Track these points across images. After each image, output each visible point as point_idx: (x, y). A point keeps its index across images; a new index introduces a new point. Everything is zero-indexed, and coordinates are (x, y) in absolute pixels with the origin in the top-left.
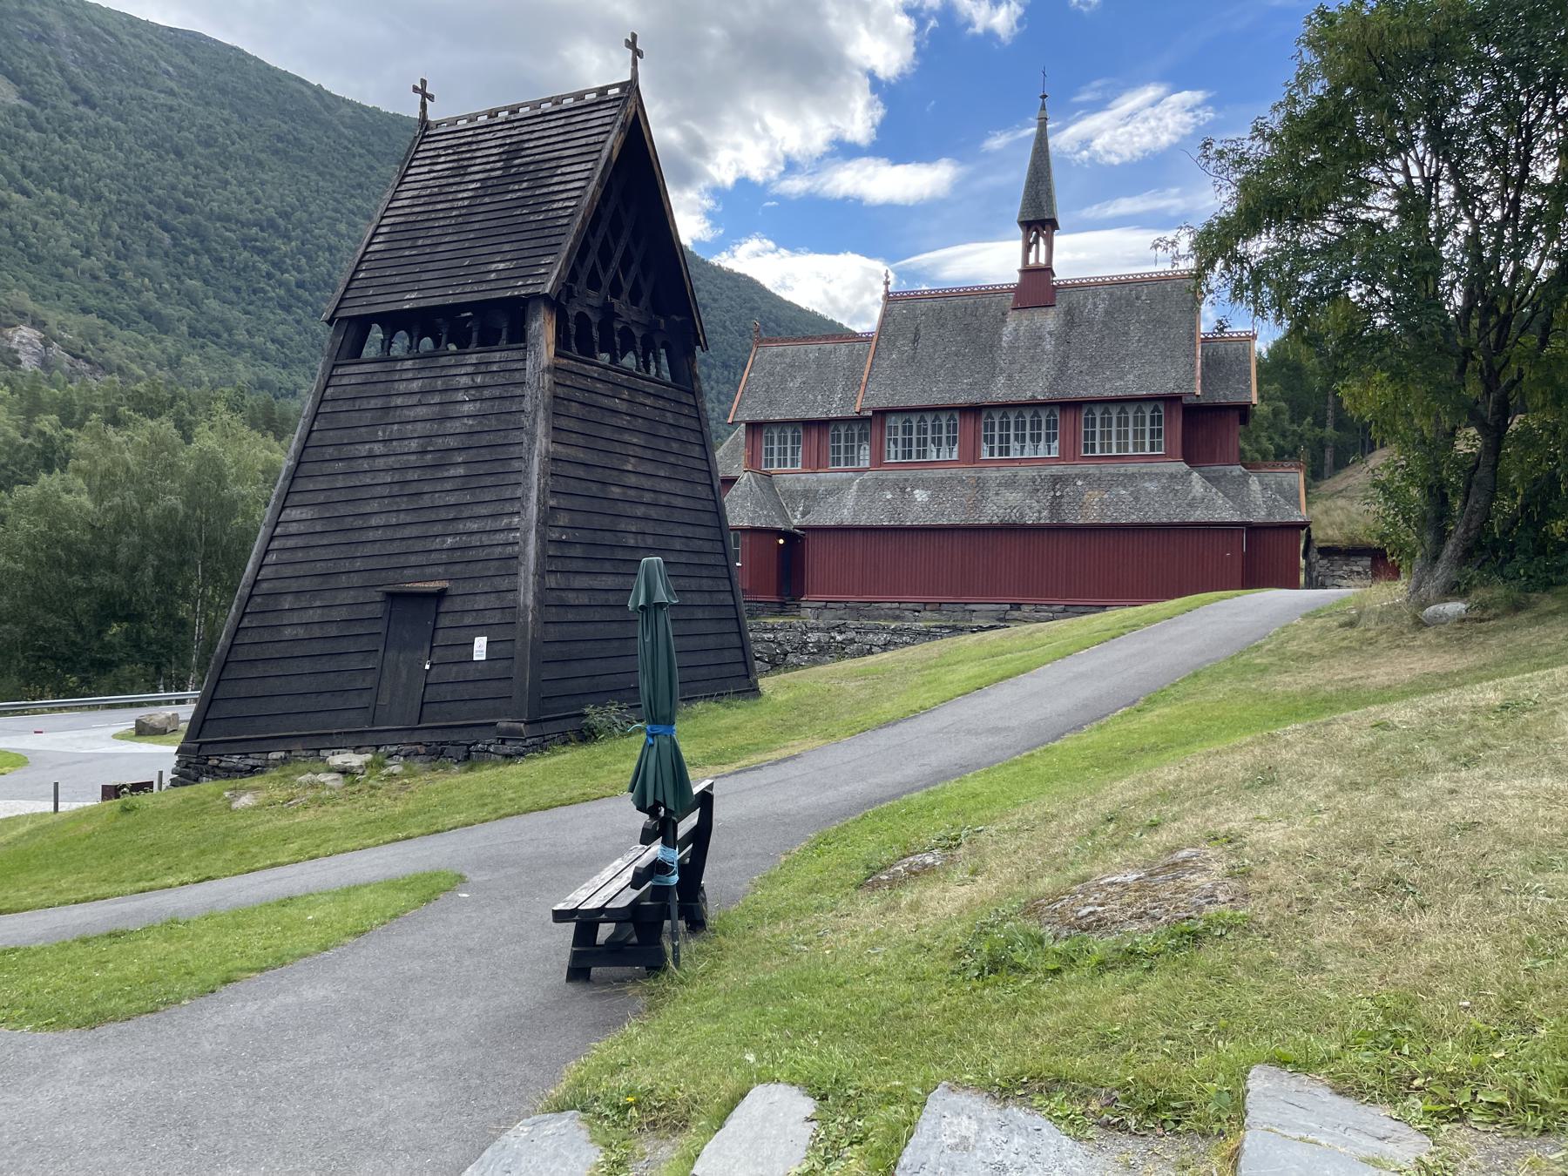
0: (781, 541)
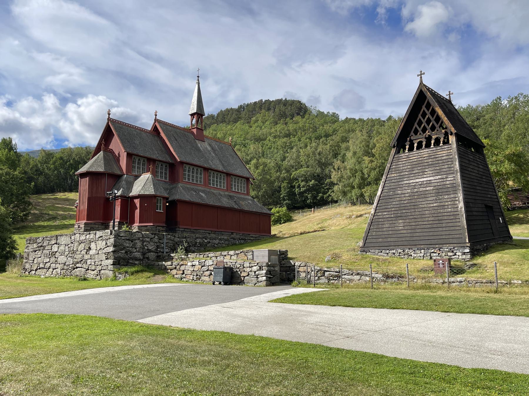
0: (167, 204)
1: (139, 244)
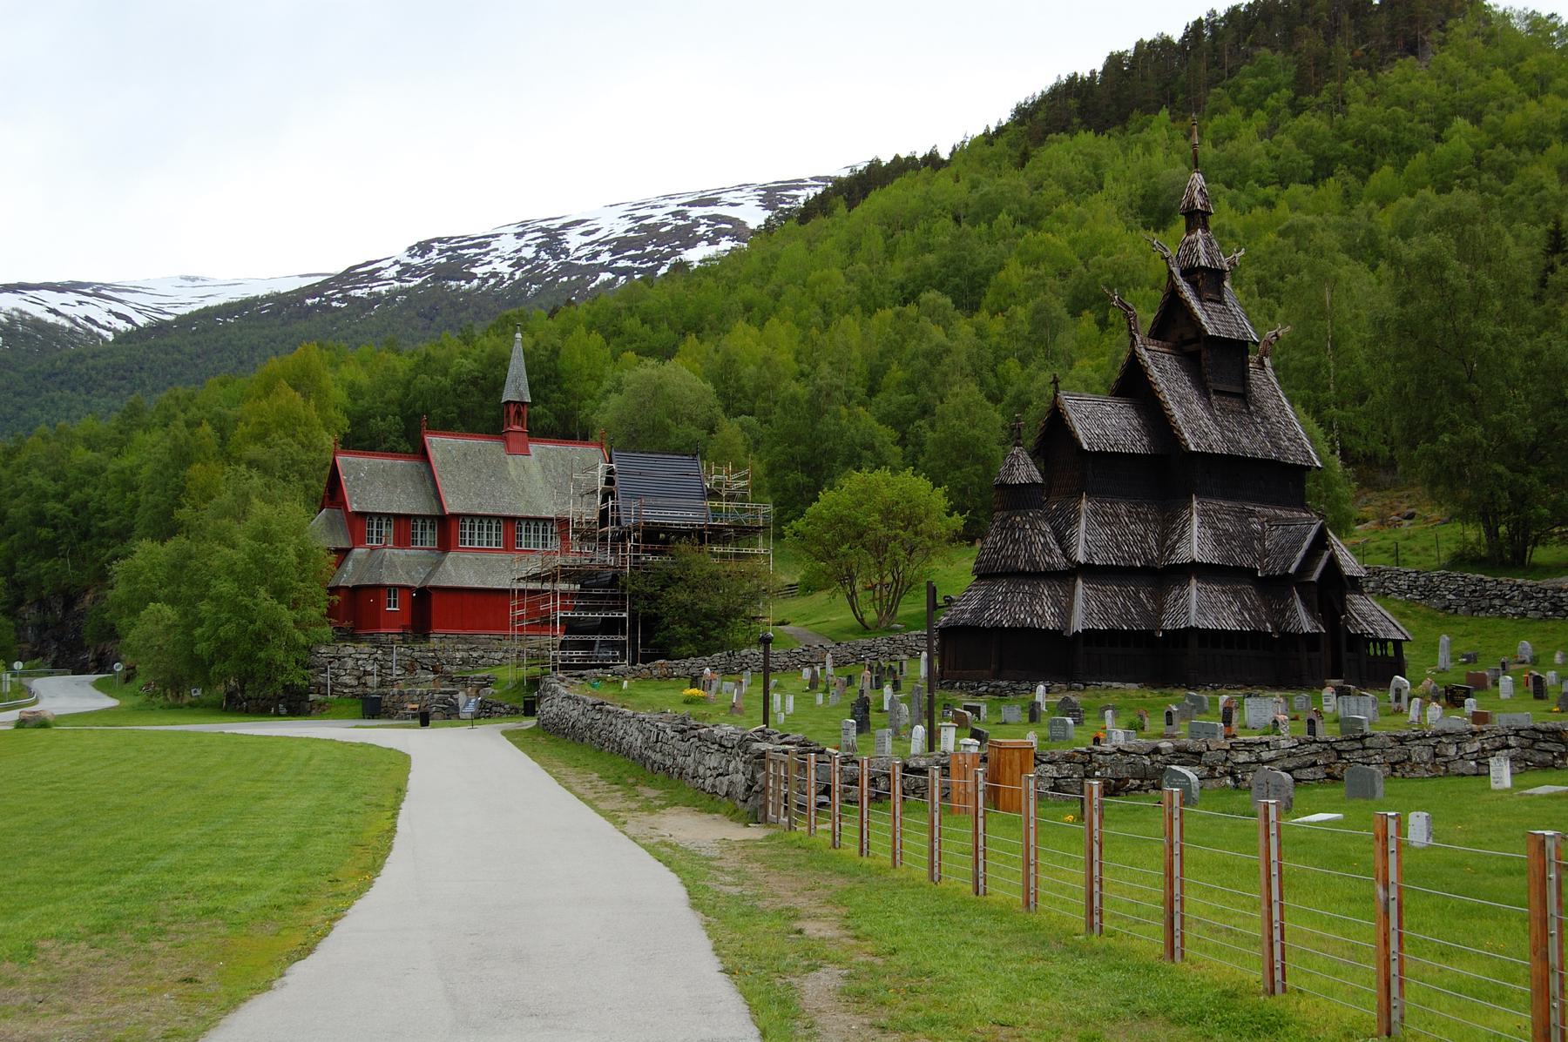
1: (350, 663)
